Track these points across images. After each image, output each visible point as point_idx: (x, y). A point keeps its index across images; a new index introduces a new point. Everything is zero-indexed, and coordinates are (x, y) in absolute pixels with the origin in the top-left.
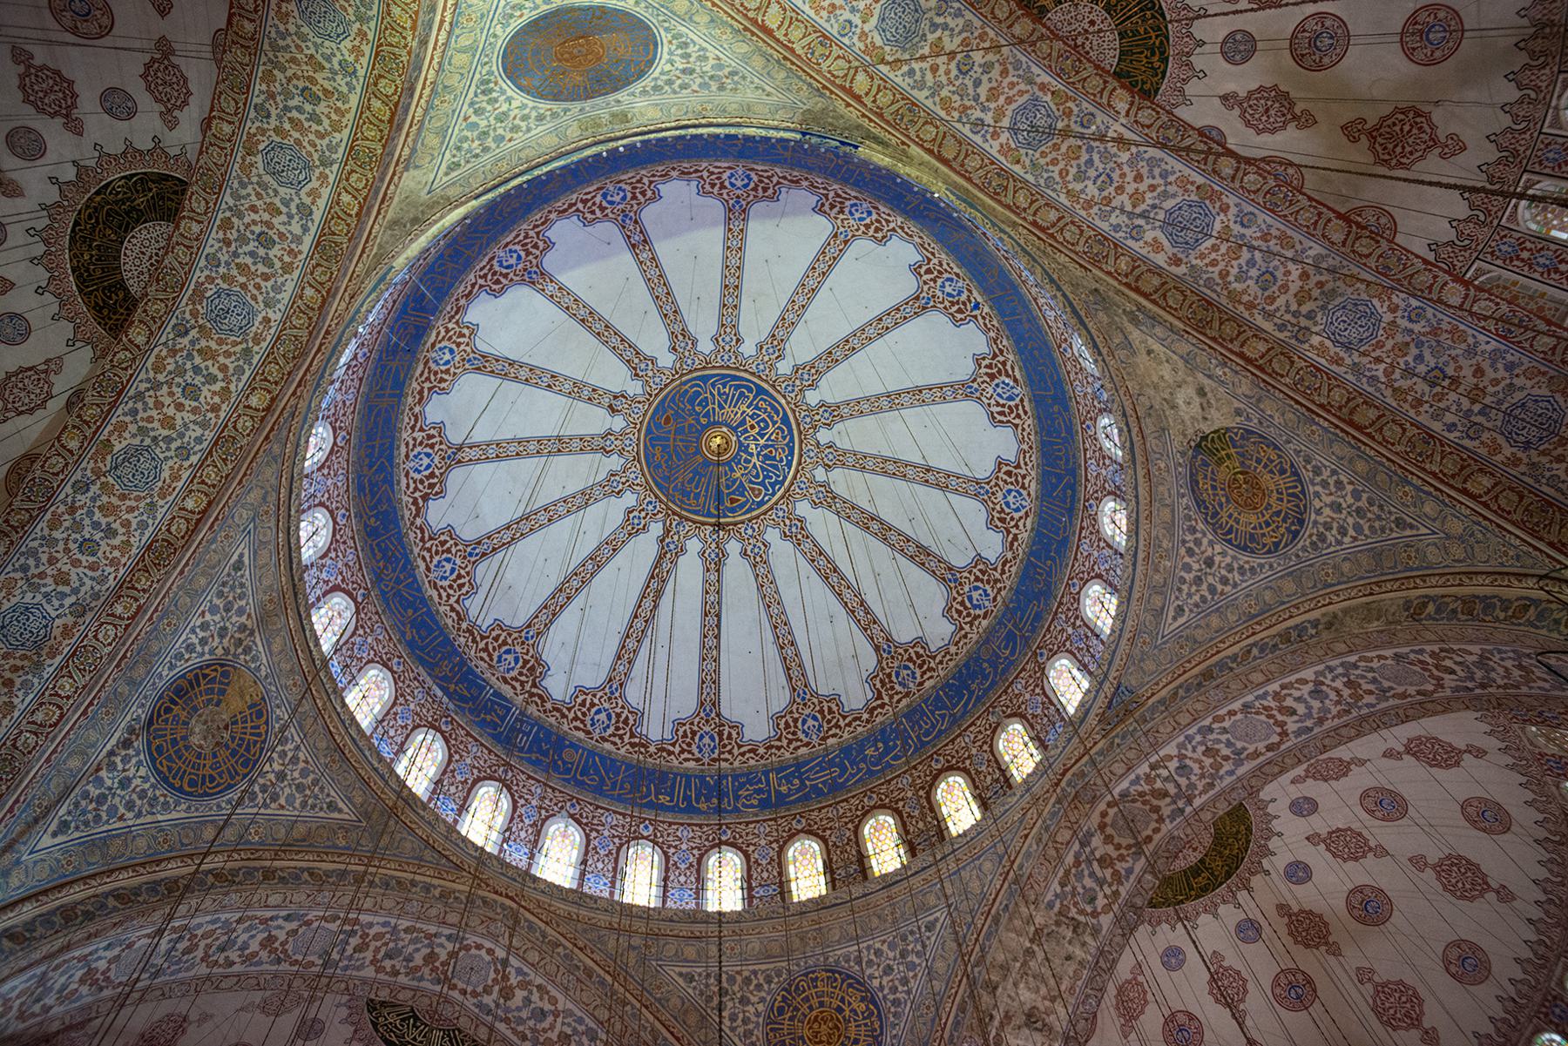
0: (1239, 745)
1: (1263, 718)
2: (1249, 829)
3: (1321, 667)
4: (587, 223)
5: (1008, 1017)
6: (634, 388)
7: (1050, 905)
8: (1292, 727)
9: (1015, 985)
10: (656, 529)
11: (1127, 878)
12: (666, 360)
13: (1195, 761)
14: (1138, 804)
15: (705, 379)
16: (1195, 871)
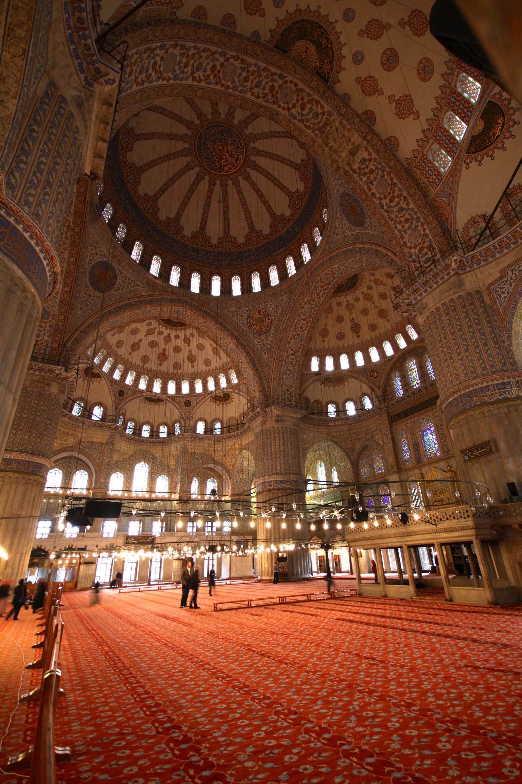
0: (239, 71)
1: (221, 74)
2: (295, 23)
3: (184, 82)
4: (159, 209)
5: (349, 164)
6: (207, 178)
7: (316, 135)
8: (222, 60)
9: (340, 157)
10: (249, 170)
11: (311, 95)
12: (197, 170)
13: (252, 82)
14: (278, 95)
15: (200, 156)
16: (318, 46)
